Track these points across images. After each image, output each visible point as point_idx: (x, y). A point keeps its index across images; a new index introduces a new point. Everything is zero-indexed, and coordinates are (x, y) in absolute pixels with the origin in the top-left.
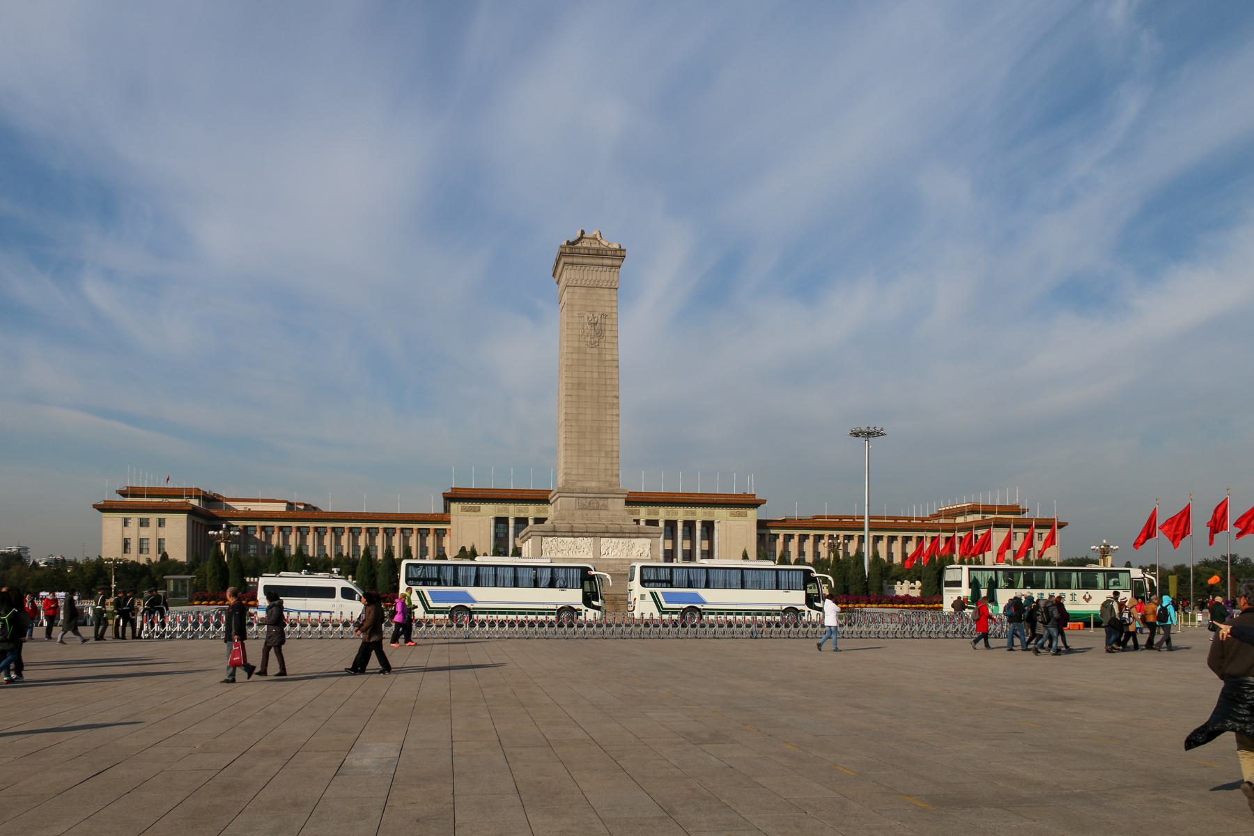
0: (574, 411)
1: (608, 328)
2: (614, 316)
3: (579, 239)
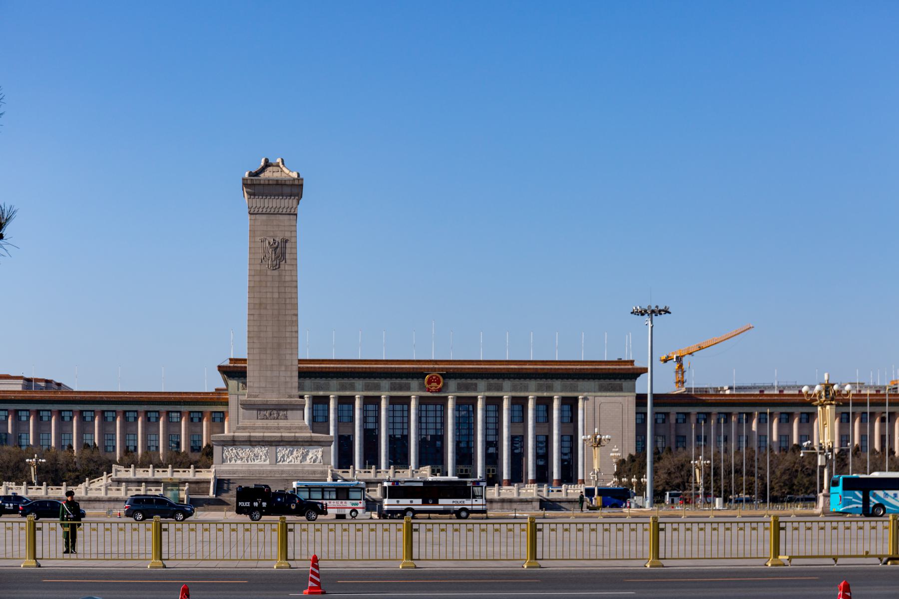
0: (256, 329)
1: (288, 251)
2: (293, 240)
3: (263, 170)
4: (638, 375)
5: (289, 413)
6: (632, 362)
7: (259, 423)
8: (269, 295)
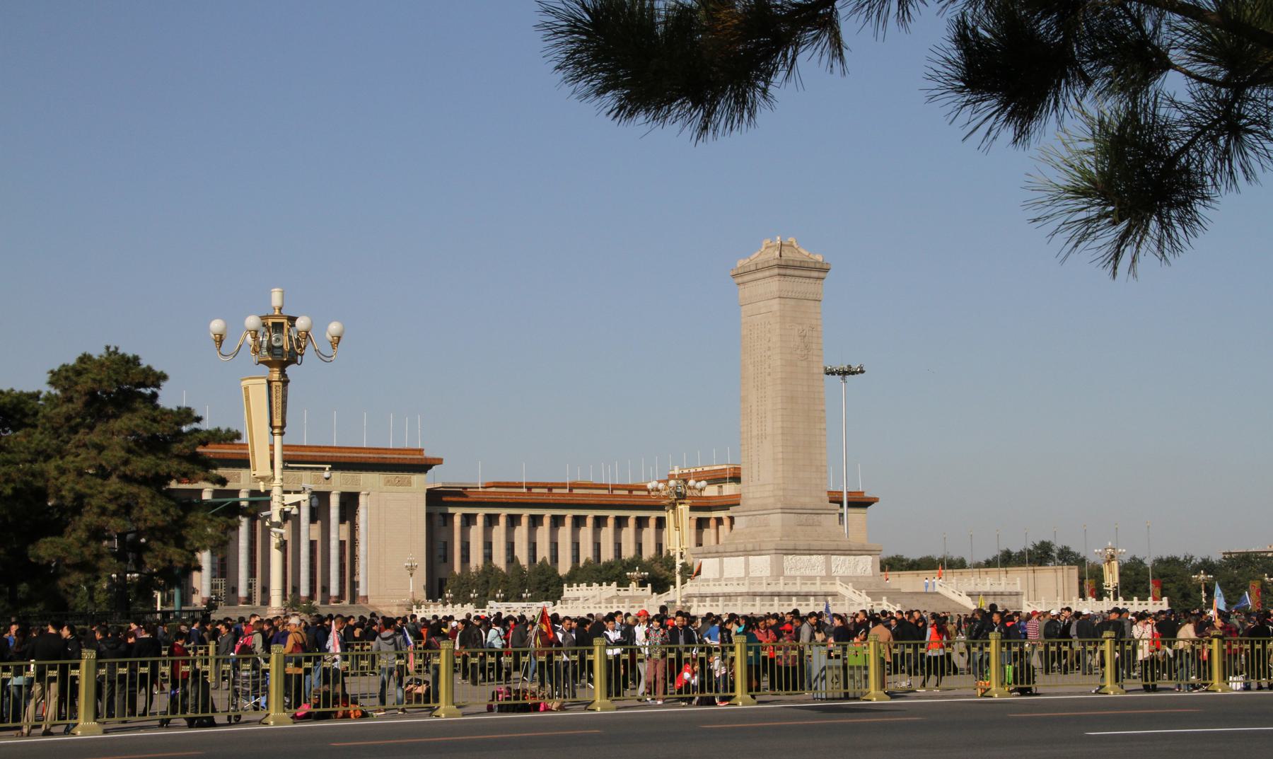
4: (430, 467)
6: (421, 451)
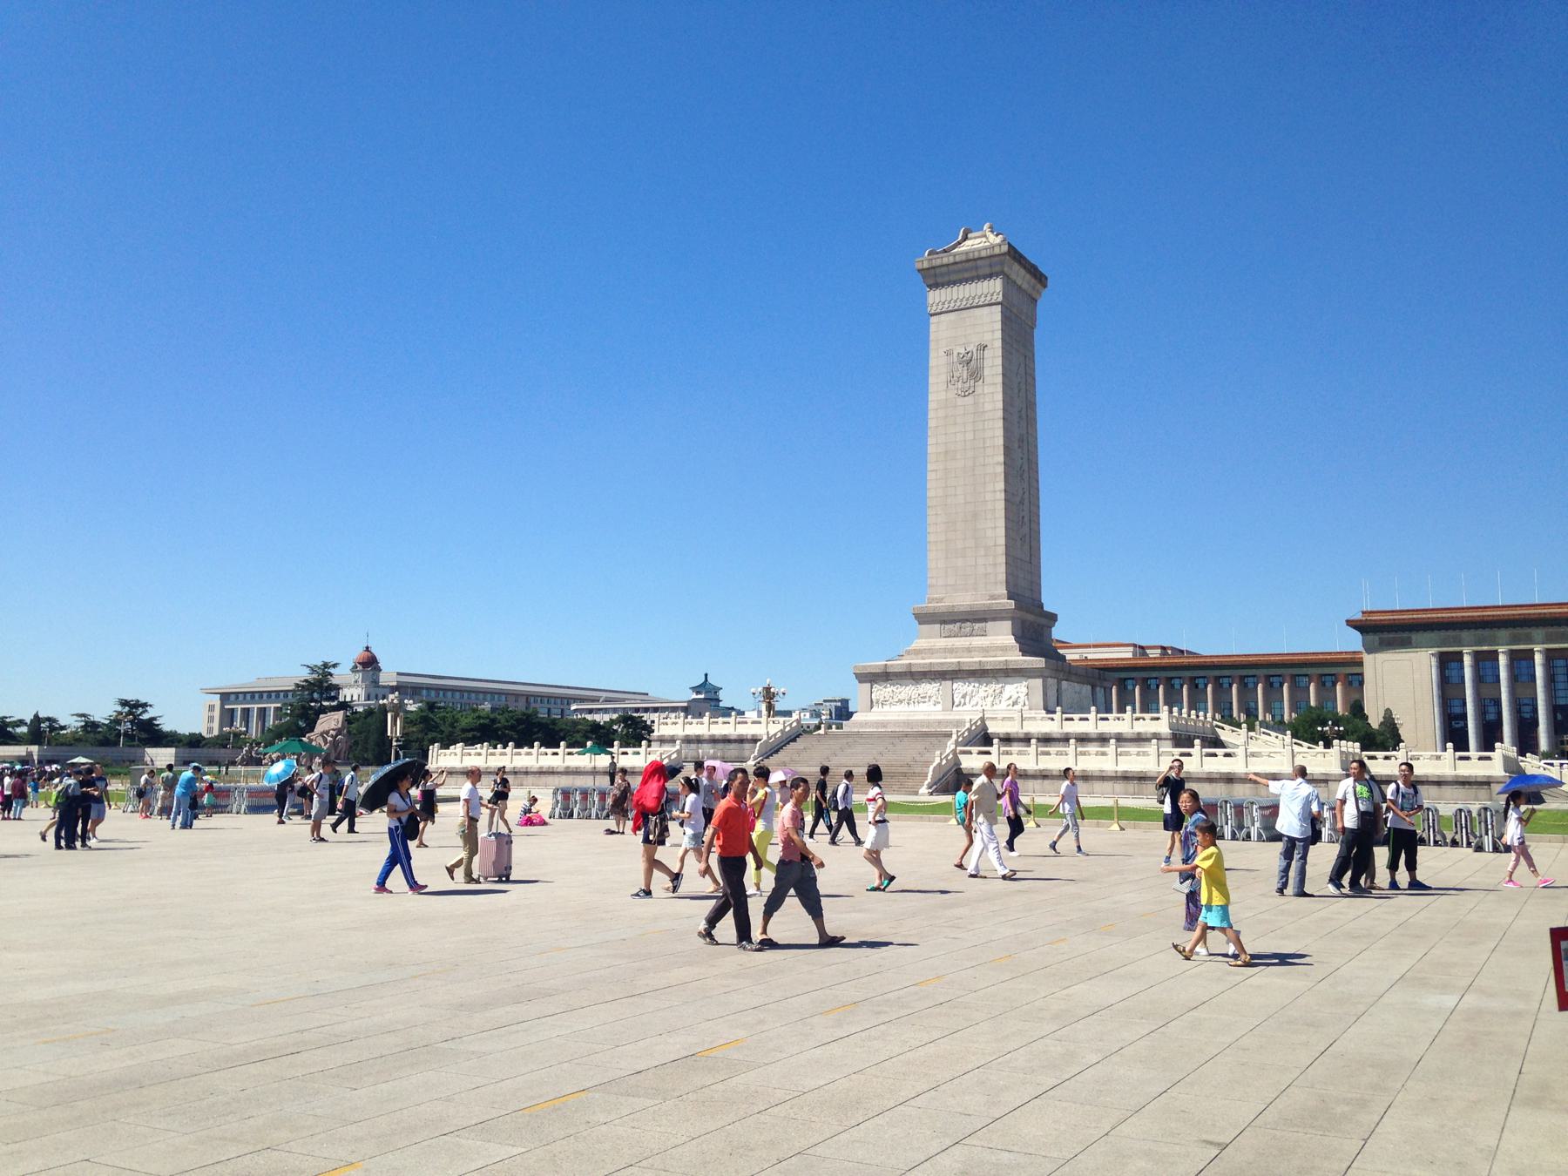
5: (990, 624)
7: (942, 643)
8: (960, 437)
